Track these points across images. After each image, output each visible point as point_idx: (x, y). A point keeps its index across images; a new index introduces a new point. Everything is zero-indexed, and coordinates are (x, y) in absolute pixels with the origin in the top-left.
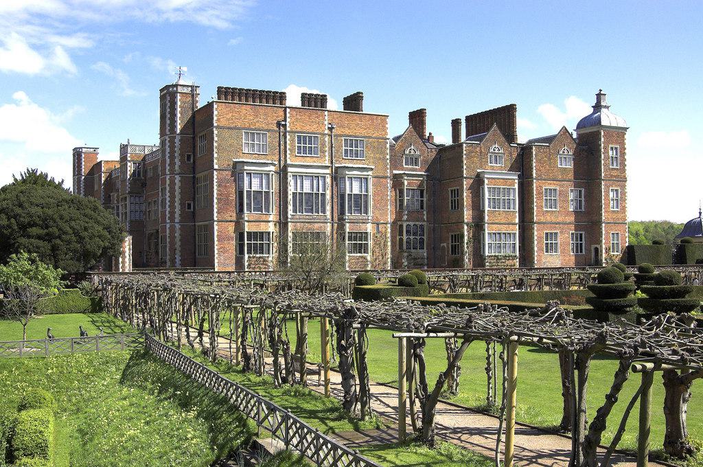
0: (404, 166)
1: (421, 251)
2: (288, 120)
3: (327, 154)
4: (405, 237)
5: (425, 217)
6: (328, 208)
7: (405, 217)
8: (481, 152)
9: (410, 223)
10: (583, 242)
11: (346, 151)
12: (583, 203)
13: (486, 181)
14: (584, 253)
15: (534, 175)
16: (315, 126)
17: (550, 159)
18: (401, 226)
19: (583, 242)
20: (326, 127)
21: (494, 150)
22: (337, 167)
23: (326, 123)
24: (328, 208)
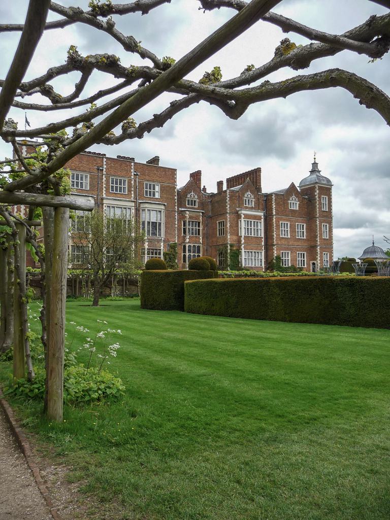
2: (105, 167)
3: (133, 192)
4: (187, 254)
5: (201, 241)
8: (239, 197)
9: (191, 244)
10: (305, 259)
11: (146, 191)
12: (305, 234)
13: (243, 216)
14: (306, 266)
15: (274, 213)
16: (125, 172)
17: (284, 203)
18: (185, 247)
19: (305, 259)
20: (133, 174)
22: (141, 203)
23: (132, 171)
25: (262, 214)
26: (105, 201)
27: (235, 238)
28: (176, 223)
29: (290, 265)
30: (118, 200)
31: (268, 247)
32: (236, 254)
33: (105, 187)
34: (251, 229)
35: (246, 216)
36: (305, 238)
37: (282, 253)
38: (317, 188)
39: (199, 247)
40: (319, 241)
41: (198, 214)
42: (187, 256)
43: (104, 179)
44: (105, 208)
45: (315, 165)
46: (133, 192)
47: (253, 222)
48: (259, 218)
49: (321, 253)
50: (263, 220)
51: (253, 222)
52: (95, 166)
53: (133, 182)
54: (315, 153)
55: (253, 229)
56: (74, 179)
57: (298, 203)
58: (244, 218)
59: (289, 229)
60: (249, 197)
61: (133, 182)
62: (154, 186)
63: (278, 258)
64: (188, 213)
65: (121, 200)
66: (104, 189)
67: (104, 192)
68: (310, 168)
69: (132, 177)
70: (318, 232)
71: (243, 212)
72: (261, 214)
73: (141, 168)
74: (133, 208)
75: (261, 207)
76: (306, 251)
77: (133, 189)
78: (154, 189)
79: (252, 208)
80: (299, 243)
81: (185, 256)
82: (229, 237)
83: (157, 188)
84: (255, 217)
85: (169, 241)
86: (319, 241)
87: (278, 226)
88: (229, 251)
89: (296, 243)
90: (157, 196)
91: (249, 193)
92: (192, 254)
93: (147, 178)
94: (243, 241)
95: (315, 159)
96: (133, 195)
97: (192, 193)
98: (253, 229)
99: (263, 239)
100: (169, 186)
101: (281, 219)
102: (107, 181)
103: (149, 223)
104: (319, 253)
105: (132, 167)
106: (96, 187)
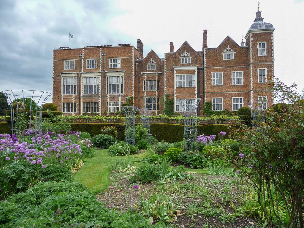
0: (148, 70)
1: (154, 110)
2: (83, 54)
3: (100, 67)
5: (157, 94)
6: (100, 91)
7: (145, 94)
9: (148, 97)
12: (243, 80)
13: (175, 72)
16: (95, 55)
18: (144, 99)
20: (101, 55)
21: (184, 55)
23: (101, 53)
24: (100, 91)
25: (196, 68)
26: (82, 75)
27: (171, 89)
28: (133, 83)
29: (223, 109)
30: (90, 73)
31: (201, 95)
32: (171, 104)
33: (83, 66)
34: (184, 81)
35: (179, 72)
36: (243, 84)
37: (214, 99)
38: (251, 35)
39: (154, 98)
40: (252, 85)
41: (154, 74)
42: (145, 106)
43: (83, 61)
44: (82, 79)
45: (259, 13)
46: (100, 67)
47: (186, 76)
48: (193, 72)
49: (255, 97)
50: (196, 73)
51: (186, 76)
52: (78, 54)
53: (101, 60)
54: (259, 3)
55: (186, 82)
56: (112, 63)
57: (234, 53)
58: (176, 74)
59: (222, 78)
60: (186, 55)
61: (101, 60)
62: (116, 60)
63: (209, 104)
64: (145, 75)
65: (92, 73)
66: (83, 68)
67: (83, 69)
68: (255, 17)
69: (101, 57)
70: (252, 78)
71: (175, 69)
72: (195, 68)
73: (107, 50)
74: (100, 77)
75: (198, 62)
76: (243, 96)
77: (101, 65)
78: (117, 62)
79: (189, 65)
80: (236, 89)
81: (144, 105)
82: (165, 90)
83: (119, 61)
84: (188, 72)
85: (127, 96)
86: (252, 85)
87: (209, 77)
88: (165, 100)
89: (230, 90)
90: (119, 66)
91: (186, 53)
92: (149, 104)
93: (112, 55)
94: (175, 92)
95: (259, 8)
96: (101, 69)
97: (152, 60)
98: (186, 82)
99: (196, 89)
100: (128, 58)
101: (213, 70)
102: (85, 63)
103: (110, 85)
104: (252, 97)
105: (101, 51)
106: (78, 67)
